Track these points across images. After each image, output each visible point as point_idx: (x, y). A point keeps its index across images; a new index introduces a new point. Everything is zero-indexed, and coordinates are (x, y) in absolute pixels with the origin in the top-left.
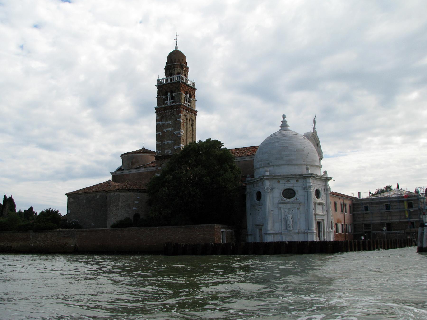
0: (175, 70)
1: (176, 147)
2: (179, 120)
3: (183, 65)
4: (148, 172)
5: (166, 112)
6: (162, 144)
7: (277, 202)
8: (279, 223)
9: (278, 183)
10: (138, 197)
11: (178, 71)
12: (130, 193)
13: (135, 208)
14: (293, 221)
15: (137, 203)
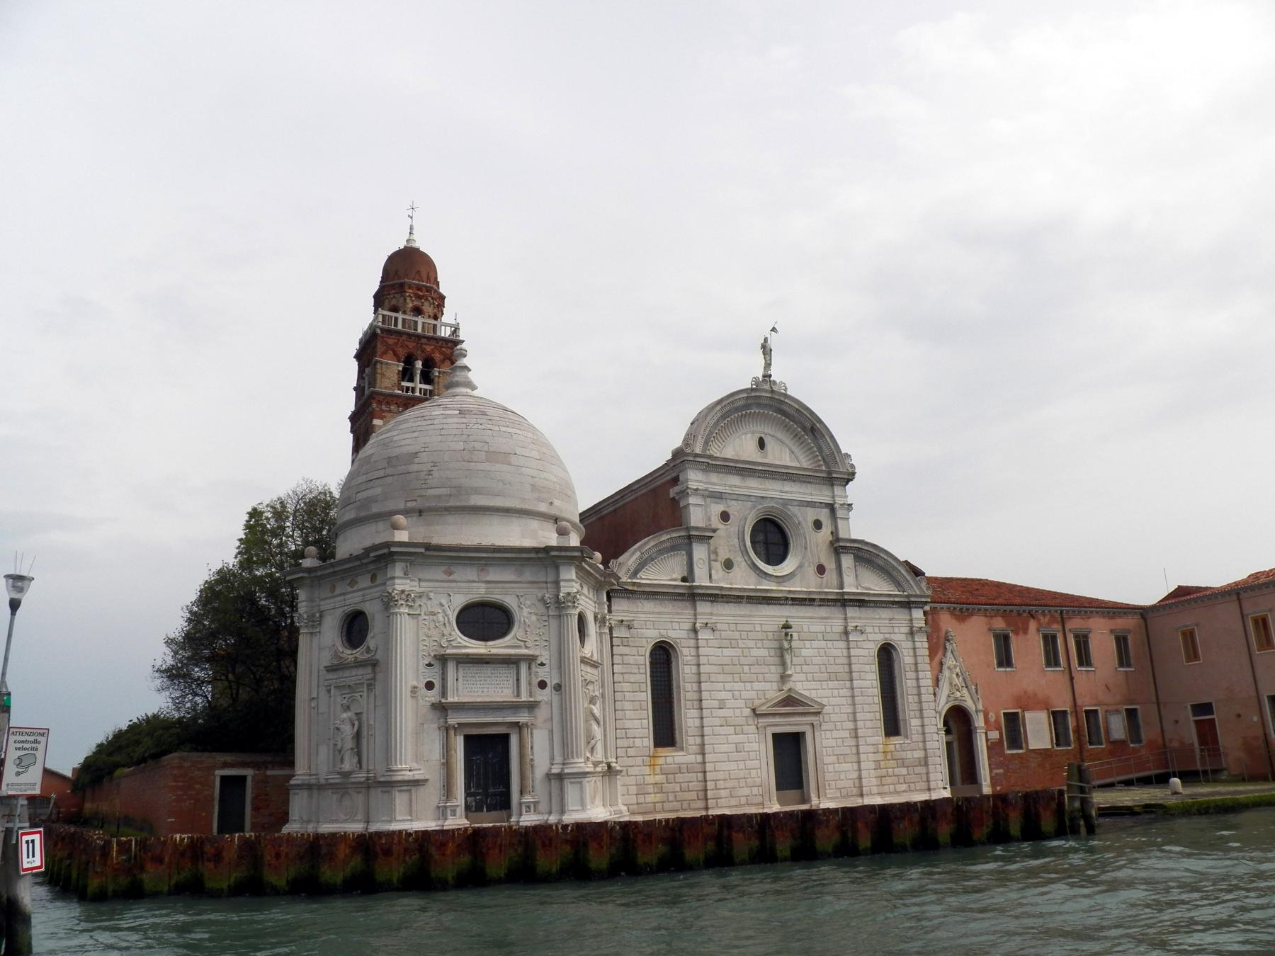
3: (404, 283)
9: (330, 595)
11: (392, 303)
14: (358, 736)
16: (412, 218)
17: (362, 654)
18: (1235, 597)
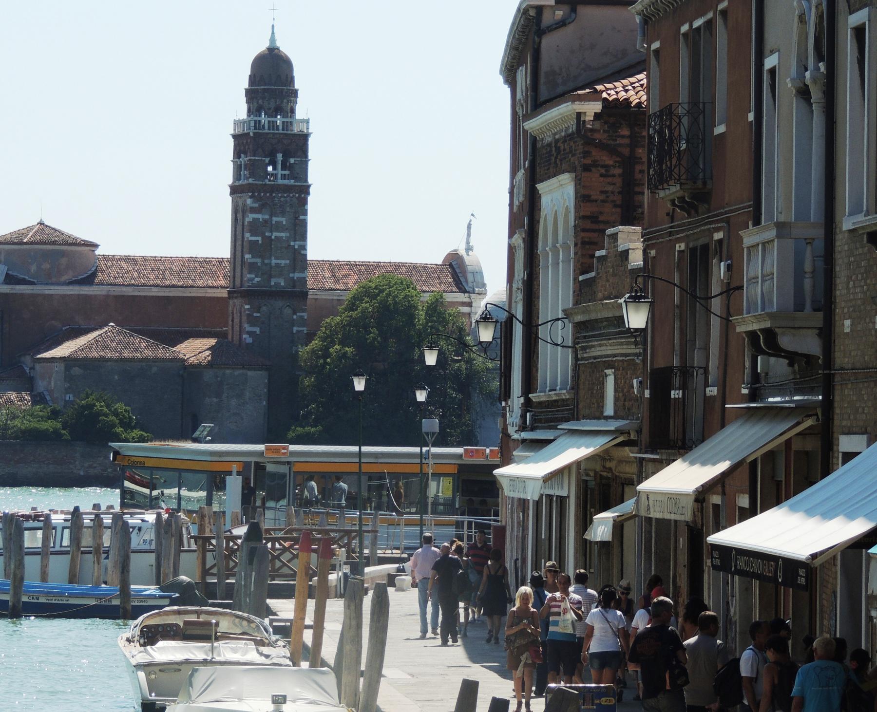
1: (297, 275)
4: (107, 296)
5: (274, 196)
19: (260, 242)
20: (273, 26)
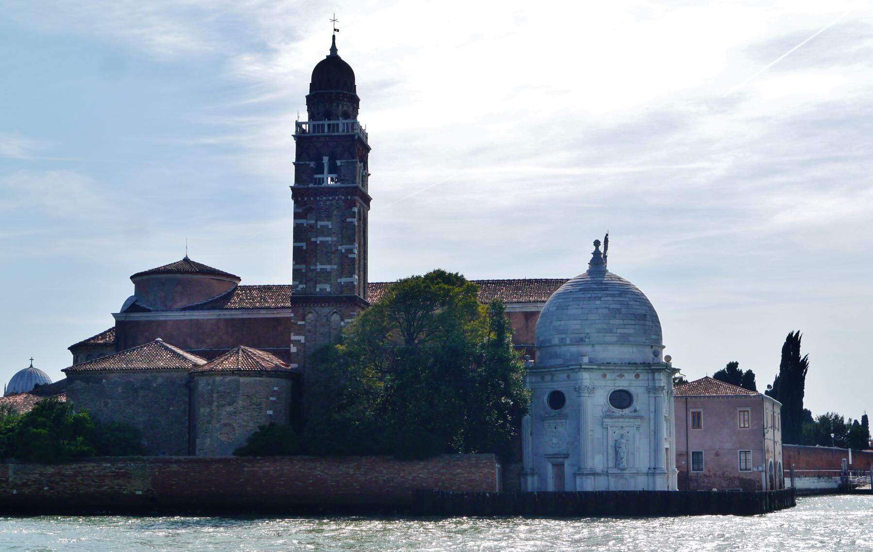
0: (338, 106)
1: (343, 280)
2: (352, 222)
4: (218, 320)
5: (319, 201)
6: (308, 269)
7: (601, 414)
8: (603, 454)
10: (276, 389)
11: (344, 109)
12: (261, 379)
13: (270, 412)
15: (274, 401)
16: (335, 30)
17: (631, 412)
18: (684, 400)
19: (305, 248)
20: (334, 37)
